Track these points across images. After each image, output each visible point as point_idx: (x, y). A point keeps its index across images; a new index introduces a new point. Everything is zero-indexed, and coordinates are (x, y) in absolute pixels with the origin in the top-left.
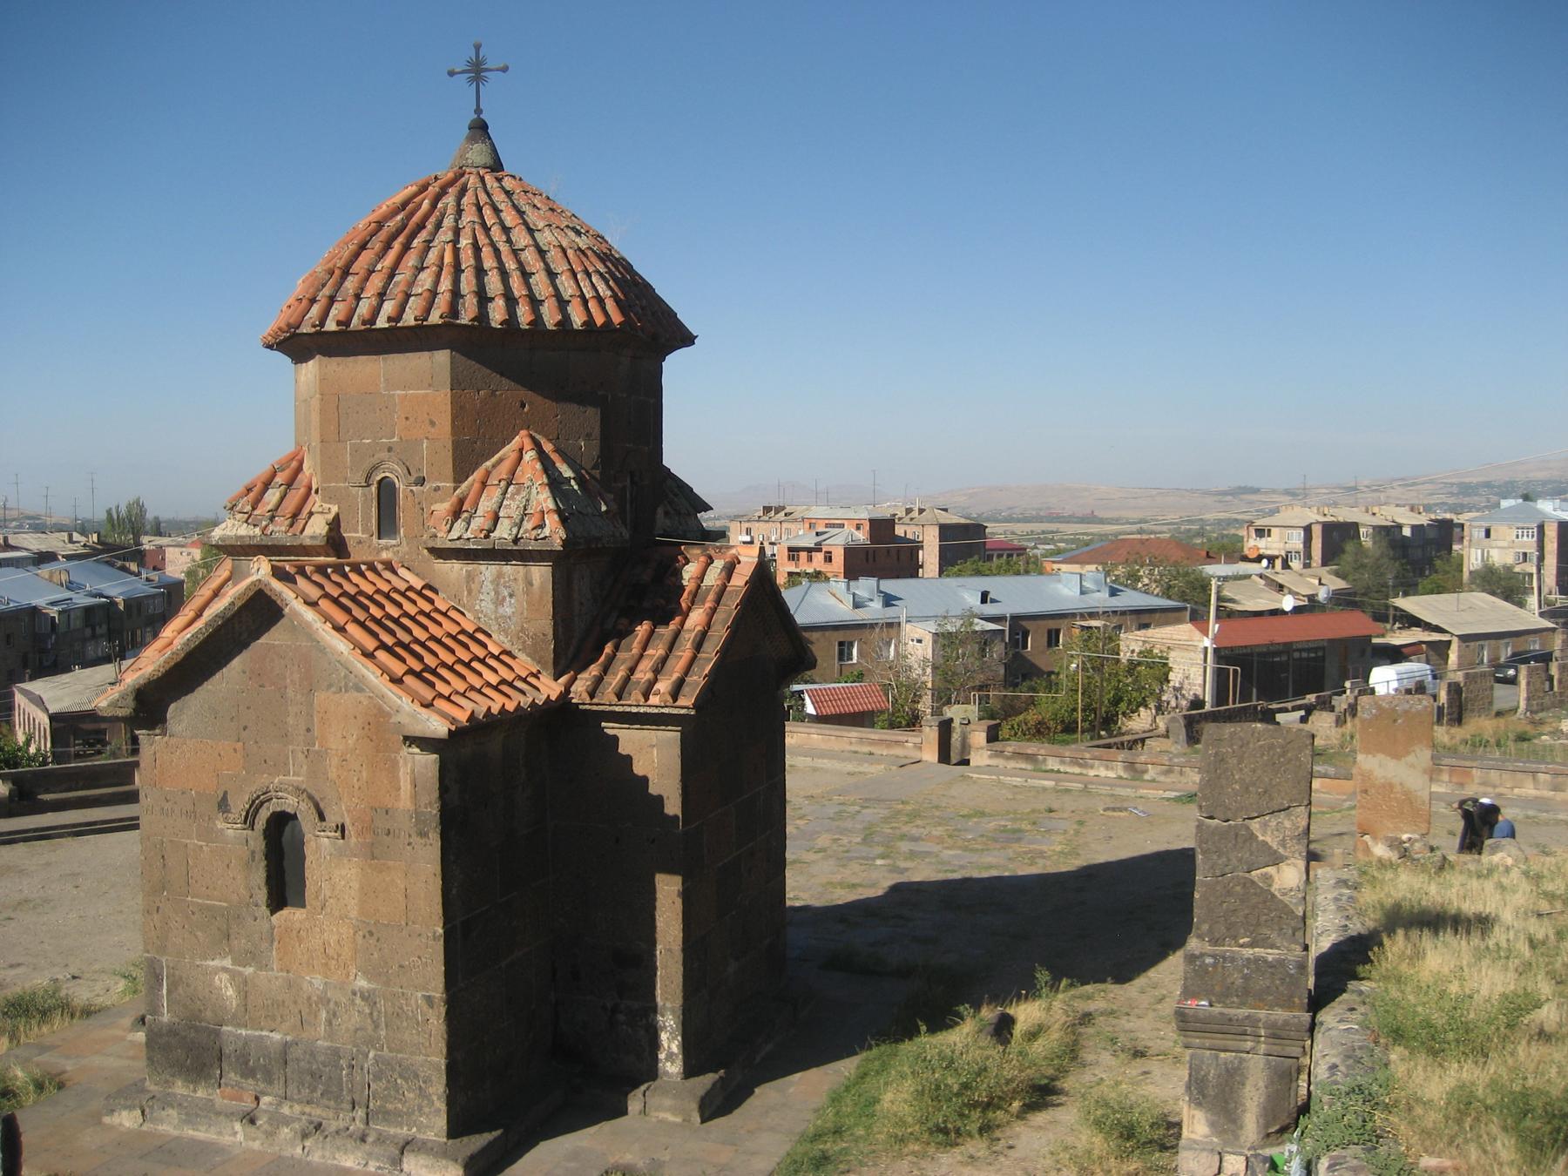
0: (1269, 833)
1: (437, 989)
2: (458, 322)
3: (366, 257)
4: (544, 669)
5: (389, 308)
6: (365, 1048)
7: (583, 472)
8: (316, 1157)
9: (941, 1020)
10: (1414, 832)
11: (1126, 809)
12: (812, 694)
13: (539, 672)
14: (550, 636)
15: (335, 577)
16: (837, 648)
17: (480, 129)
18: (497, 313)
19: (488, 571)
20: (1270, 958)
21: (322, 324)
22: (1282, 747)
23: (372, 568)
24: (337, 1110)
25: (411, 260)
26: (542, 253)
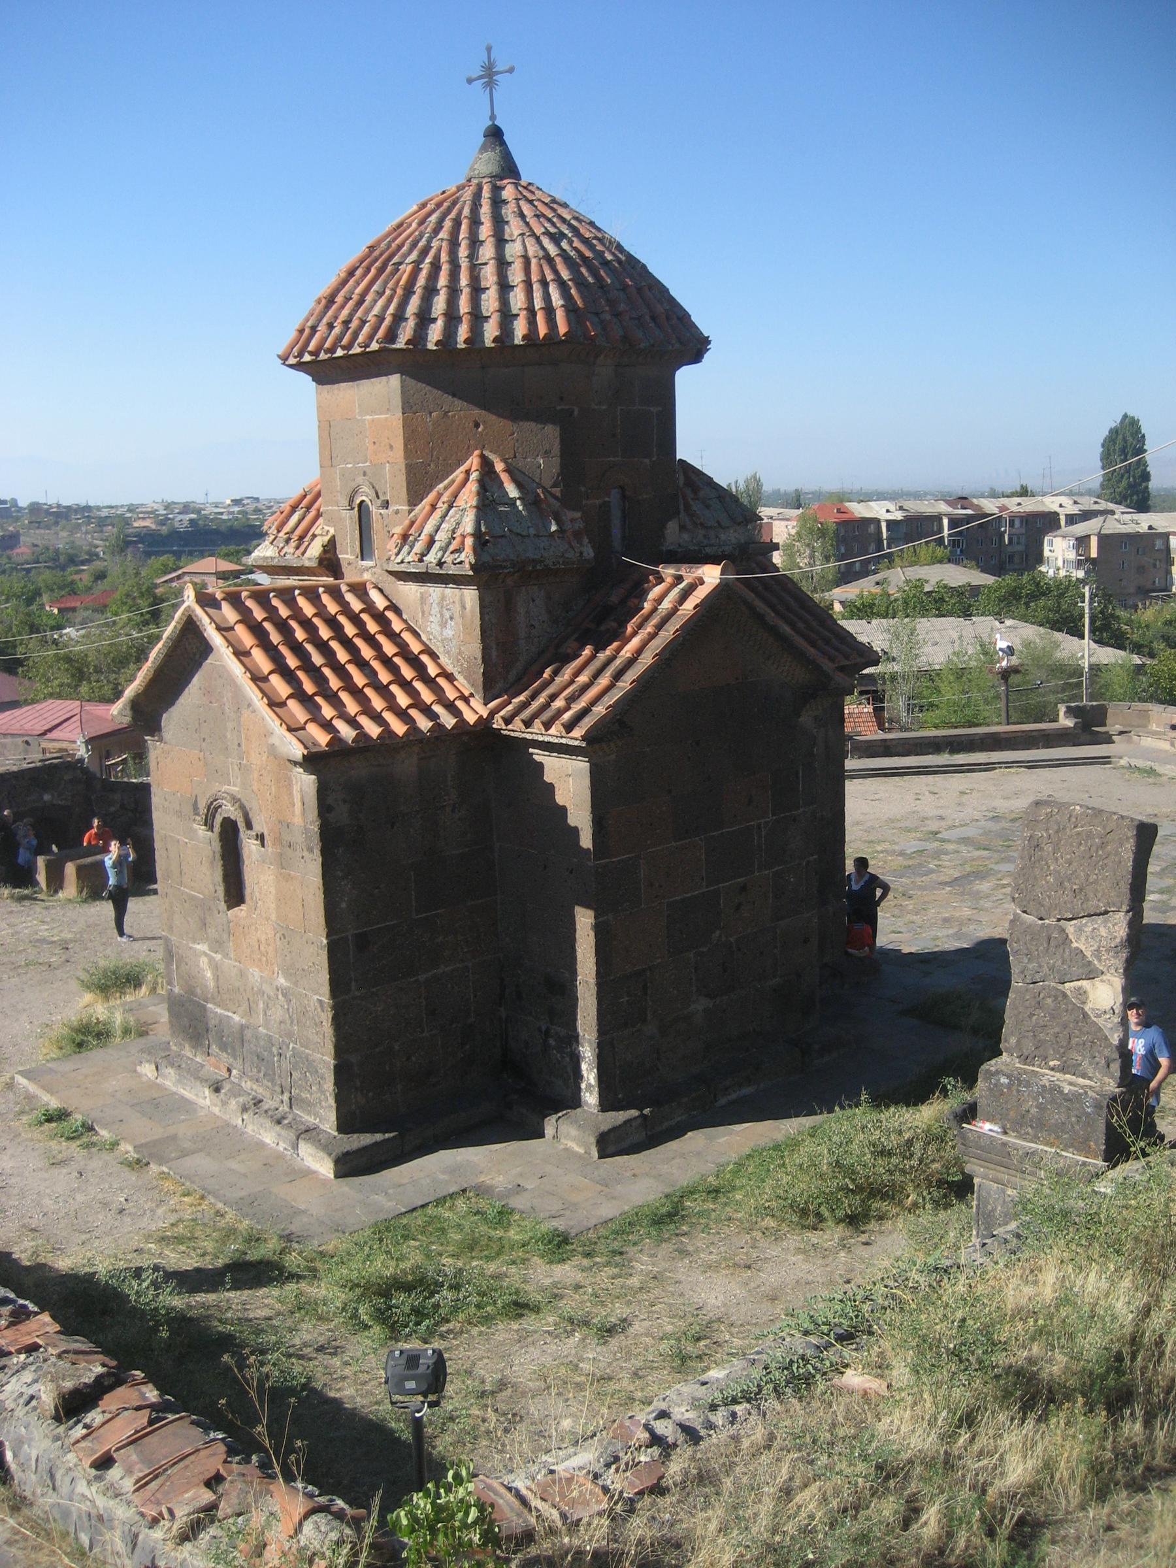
0: (1083, 939)
2: (394, 346)
4: (477, 692)
6: (286, 1040)
7: (539, 491)
8: (250, 1129)
13: (472, 695)
17: (495, 135)
19: (435, 592)
20: (1067, 1089)
26: (502, 264)
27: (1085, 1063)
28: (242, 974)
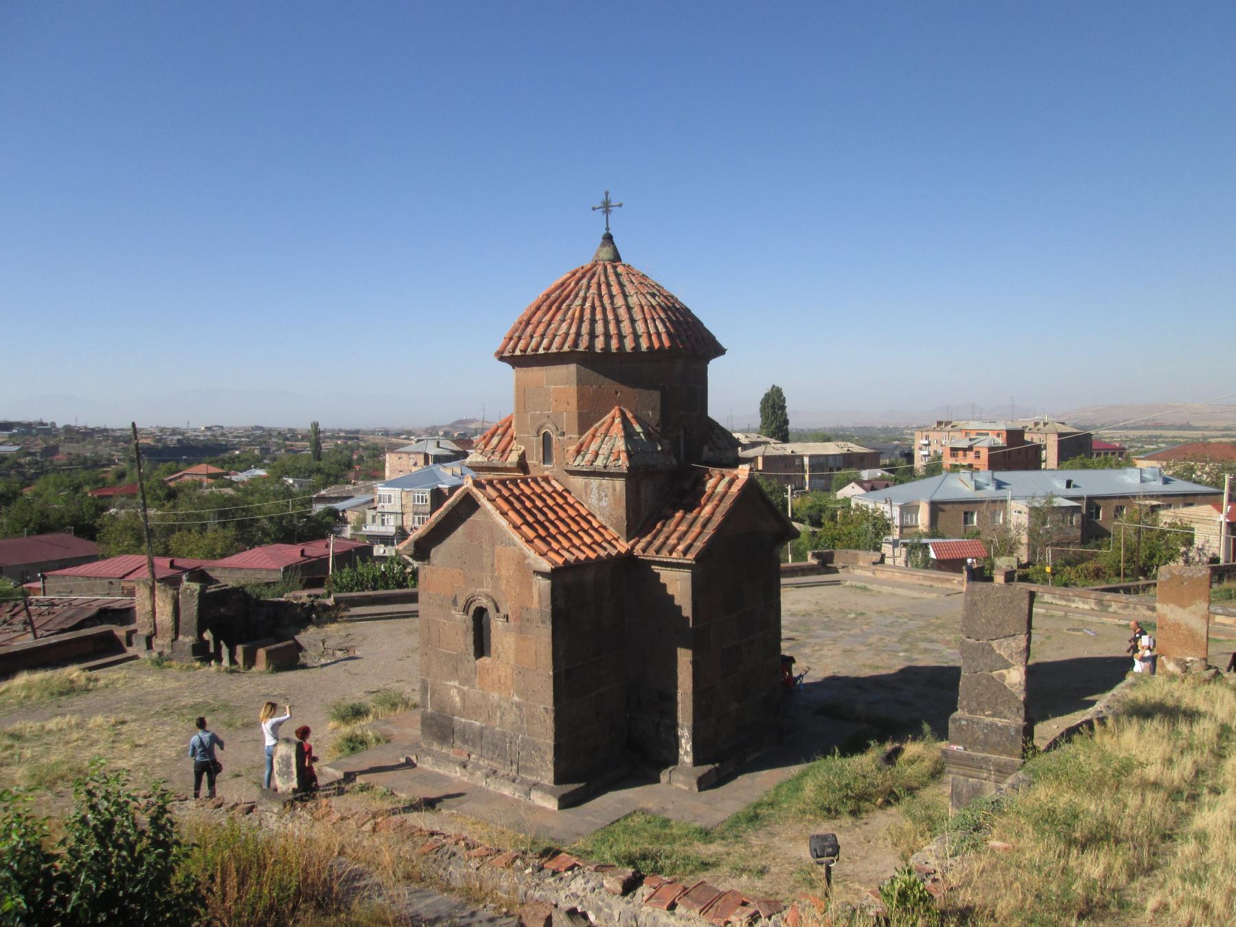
1: (550, 704)
3: (539, 313)
4: (622, 536)
5: (545, 342)
6: (516, 733)
8: (492, 788)
9: (855, 746)
10: (1197, 656)
11: (1081, 630)
12: (935, 546)
14: (625, 519)
15: (510, 486)
16: (963, 515)
17: (608, 238)
18: (599, 344)
19: (595, 482)
20: (1000, 724)
21: (514, 351)
22: (1010, 598)
23: (535, 480)
24: (504, 765)
25: (559, 317)
26: (629, 309)
27: (1006, 711)
28: (484, 696)
